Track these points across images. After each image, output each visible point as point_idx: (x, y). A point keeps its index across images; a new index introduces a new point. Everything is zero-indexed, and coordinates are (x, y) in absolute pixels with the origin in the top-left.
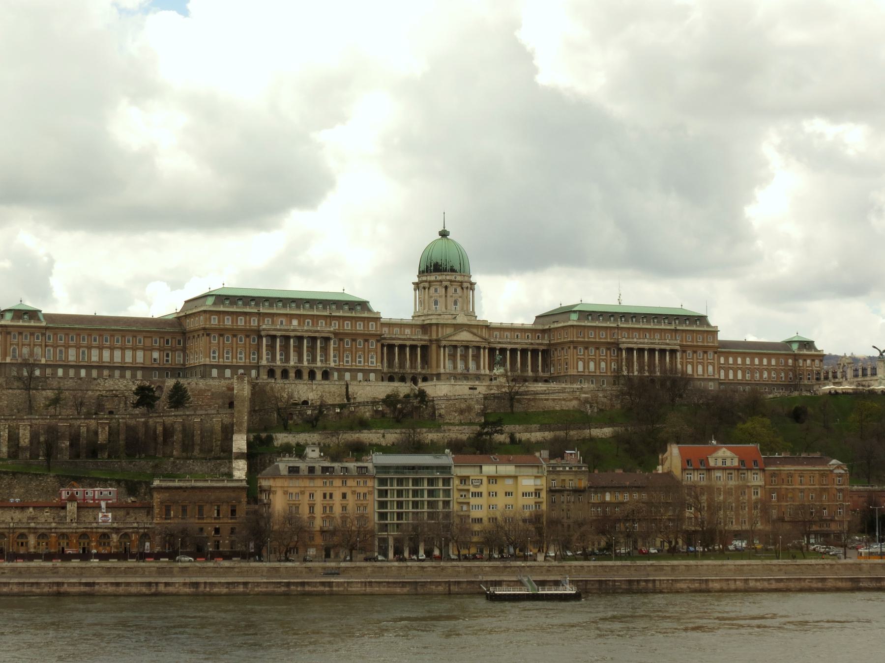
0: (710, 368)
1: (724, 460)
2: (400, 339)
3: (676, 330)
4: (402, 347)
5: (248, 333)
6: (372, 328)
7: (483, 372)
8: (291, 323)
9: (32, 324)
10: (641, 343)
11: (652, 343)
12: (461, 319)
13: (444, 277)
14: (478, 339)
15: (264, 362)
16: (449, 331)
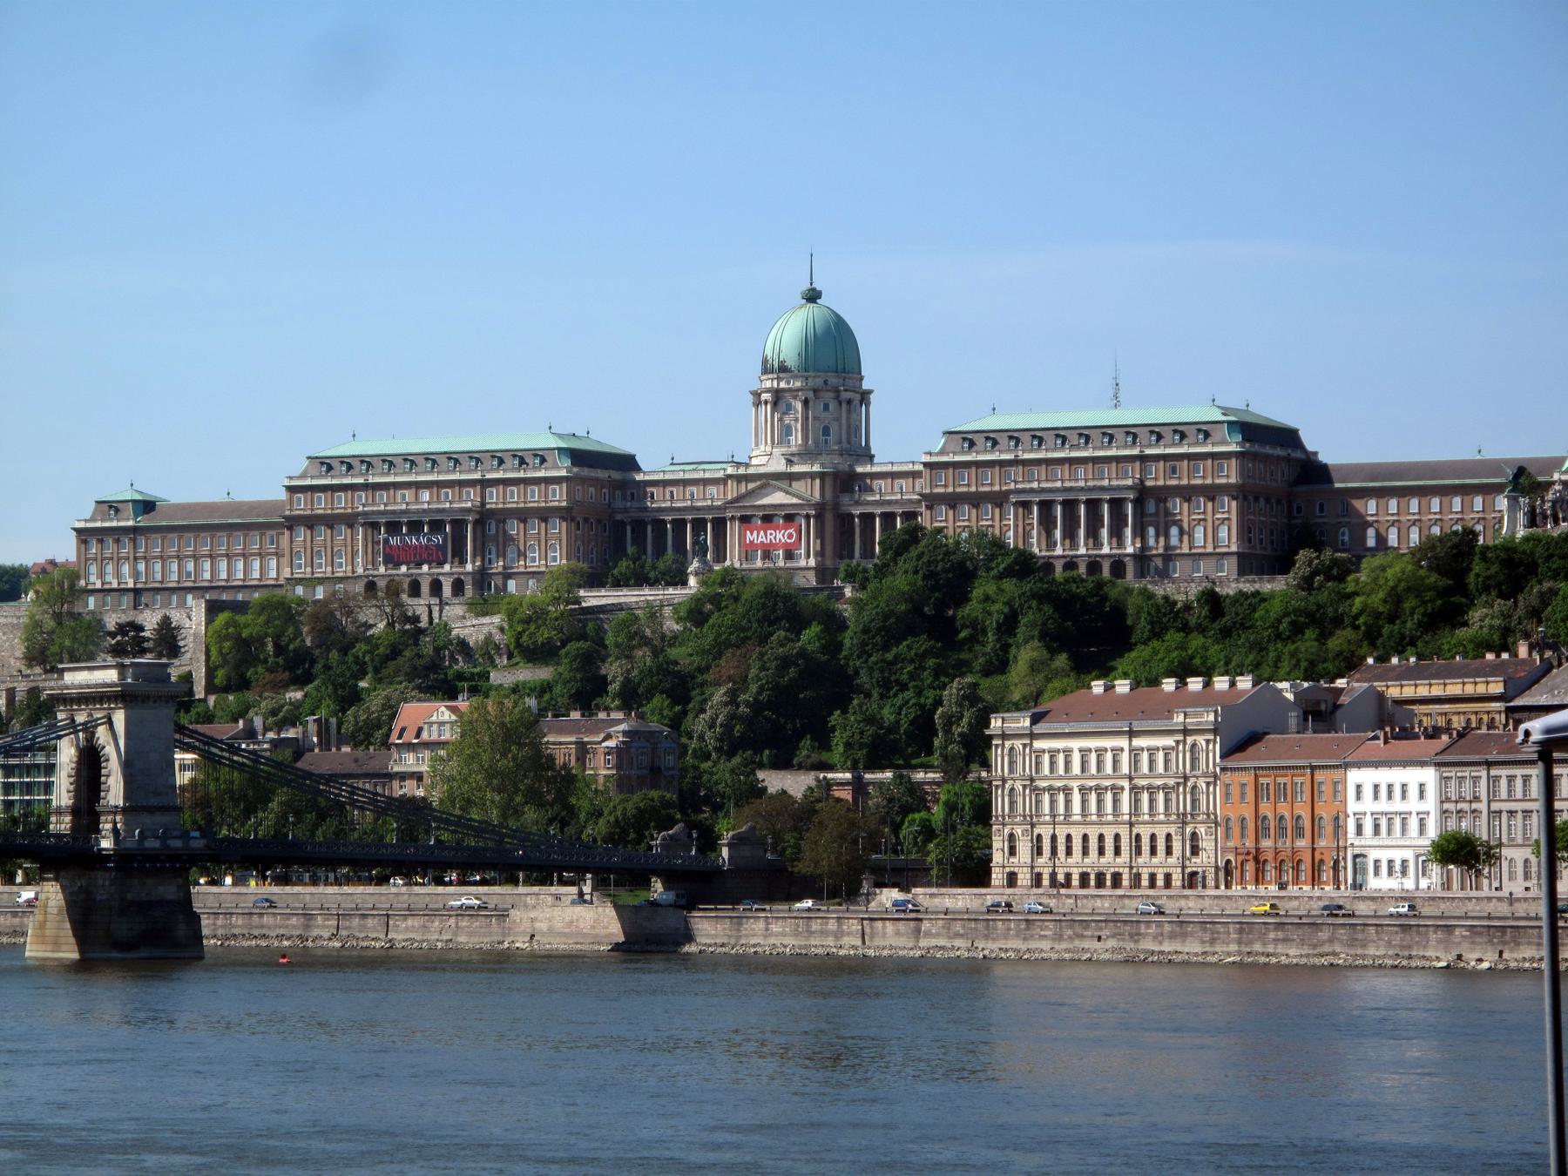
0: (1223, 533)
1: (441, 724)
2: (672, 509)
3: (1143, 458)
4: (679, 525)
5: (350, 520)
6: (558, 497)
7: (803, 563)
8: (417, 501)
9: (114, 524)
10: (1043, 490)
11: (1071, 489)
12: (779, 466)
13: (768, 384)
14: (795, 501)
15: (360, 571)
16: (751, 486)
